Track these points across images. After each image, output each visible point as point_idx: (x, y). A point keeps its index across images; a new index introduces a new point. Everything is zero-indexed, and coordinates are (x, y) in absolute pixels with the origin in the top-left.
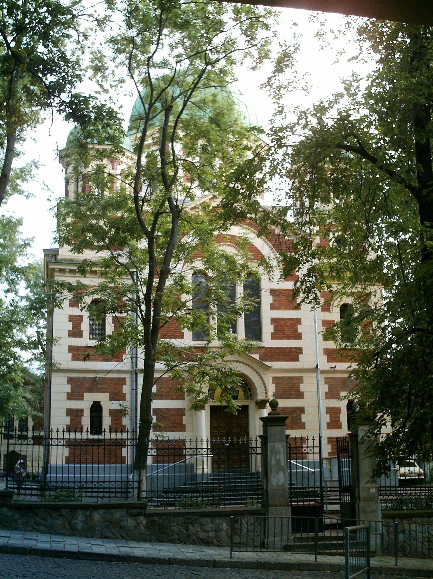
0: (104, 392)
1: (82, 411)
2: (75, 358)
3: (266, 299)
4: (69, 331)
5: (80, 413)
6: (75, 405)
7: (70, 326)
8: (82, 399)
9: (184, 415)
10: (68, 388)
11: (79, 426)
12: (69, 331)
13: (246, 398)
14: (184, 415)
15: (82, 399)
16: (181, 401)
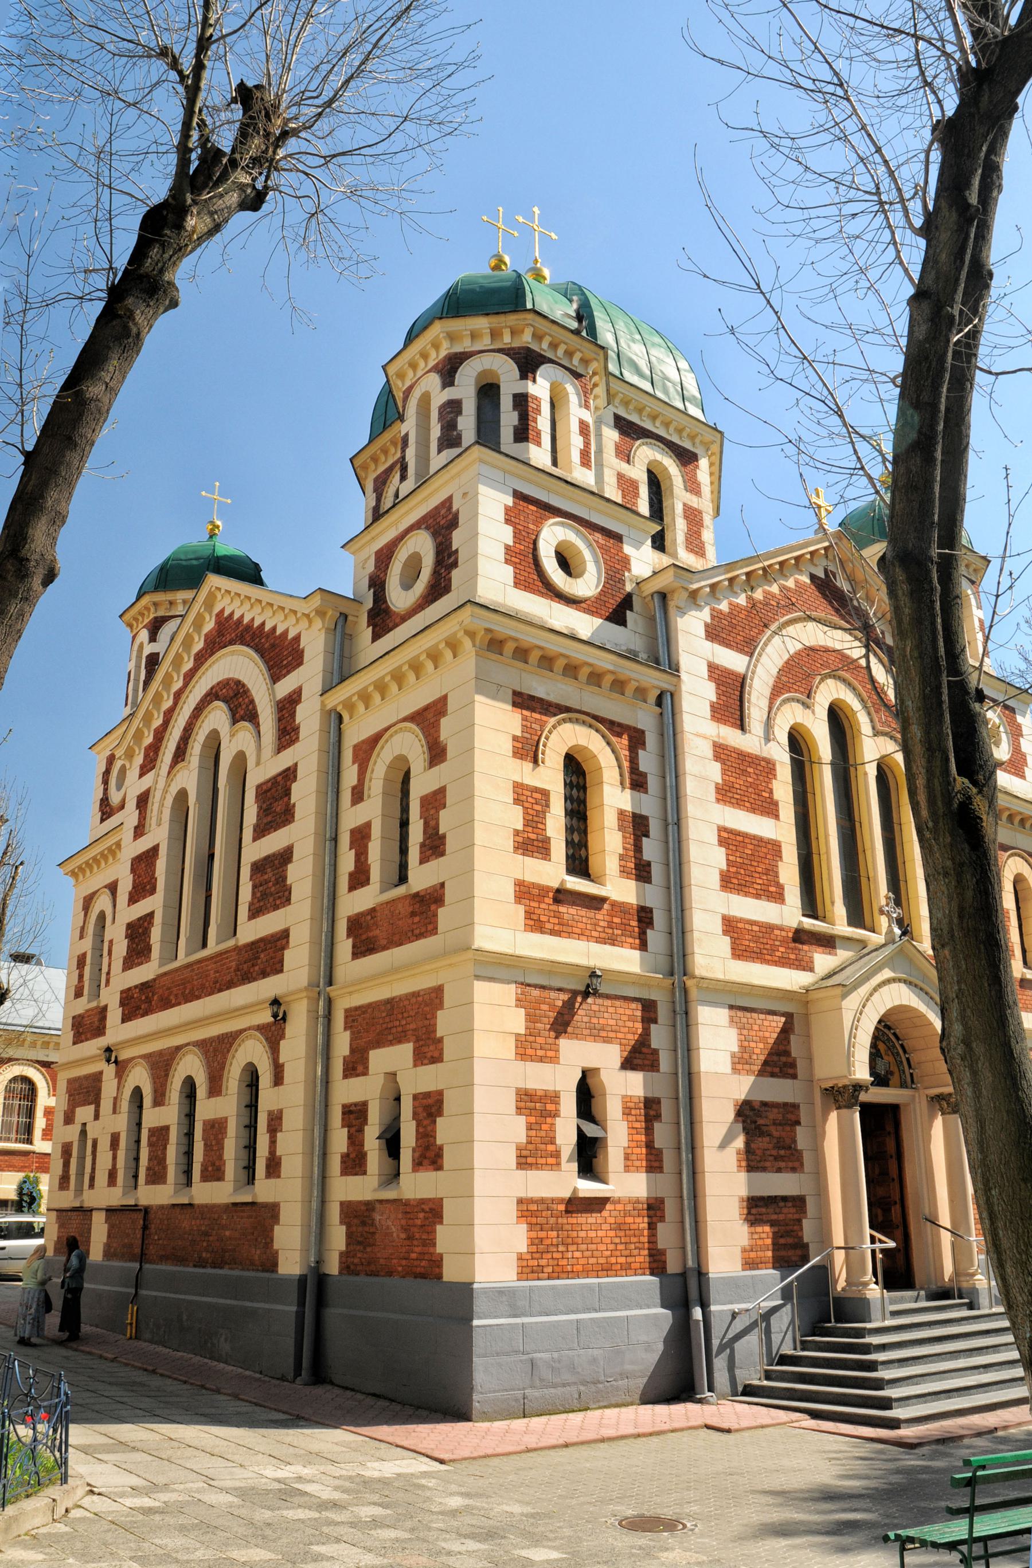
0: (607, 1040)
1: (554, 1097)
2: (535, 924)
4: (517, 833)
5: (550, 1107)
6: (539, 1077)
7: (515, 818)
8: (554, 1060)
9: (798, 1123)
10: (517, 1021)
11: (551, 1148)
12: (517, 833)
13: (903, 1085)
14: (798, 1123)
15: (554, 1060)
16: (789, 1081)
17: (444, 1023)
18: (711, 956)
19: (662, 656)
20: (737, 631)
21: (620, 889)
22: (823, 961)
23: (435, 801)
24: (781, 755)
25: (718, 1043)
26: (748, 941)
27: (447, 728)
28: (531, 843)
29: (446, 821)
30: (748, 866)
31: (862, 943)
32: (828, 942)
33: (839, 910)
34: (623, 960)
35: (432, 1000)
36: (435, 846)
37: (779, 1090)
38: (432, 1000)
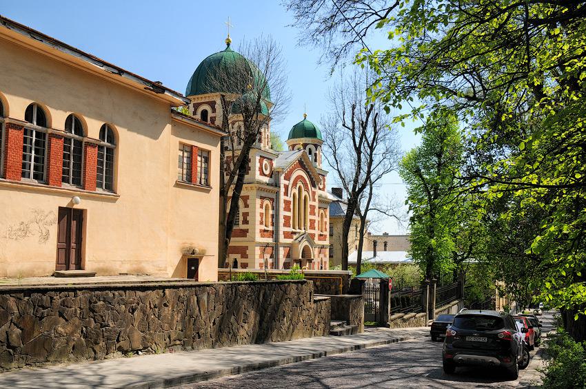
3: (309, 210)
17: (248, 252)
18: (282, 240)
19: (277, 185)
20: (287, 178)
21: (270, 228)
22: (295, 237)
23: (246, 215)
24: (292, 199)
25: (282, 252)
26: (287, 235)
27: (249, 202)
28: (261, 223)
29: (248, 218)
30: (286, 224)
31: (300, 233)
32: (295, 233)
33: (297, 227)
34: (270, 240)
35: (246, 248)
36: (245, 222)
37: (289, 260)
38: (246, 248)
